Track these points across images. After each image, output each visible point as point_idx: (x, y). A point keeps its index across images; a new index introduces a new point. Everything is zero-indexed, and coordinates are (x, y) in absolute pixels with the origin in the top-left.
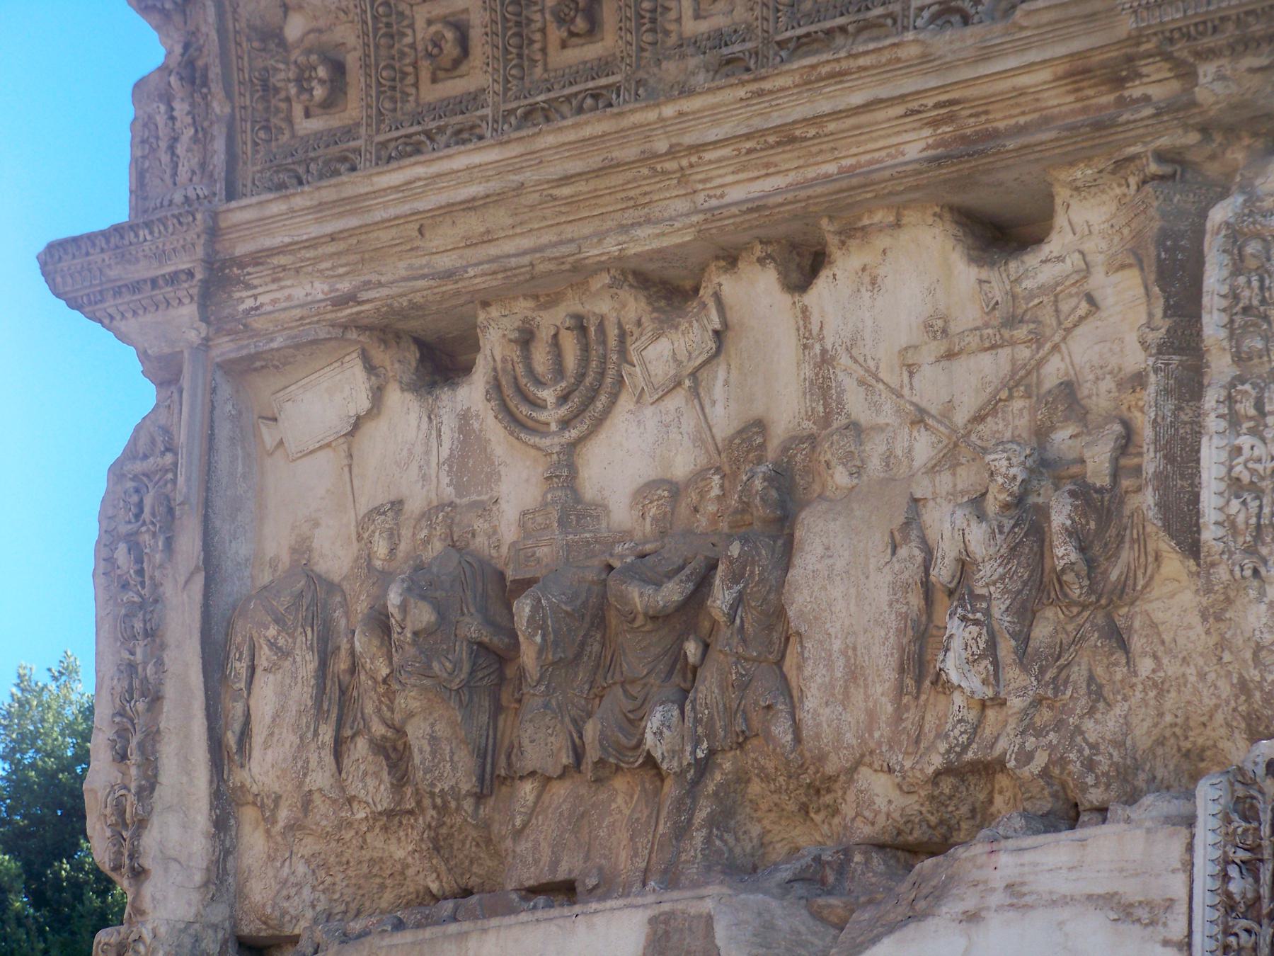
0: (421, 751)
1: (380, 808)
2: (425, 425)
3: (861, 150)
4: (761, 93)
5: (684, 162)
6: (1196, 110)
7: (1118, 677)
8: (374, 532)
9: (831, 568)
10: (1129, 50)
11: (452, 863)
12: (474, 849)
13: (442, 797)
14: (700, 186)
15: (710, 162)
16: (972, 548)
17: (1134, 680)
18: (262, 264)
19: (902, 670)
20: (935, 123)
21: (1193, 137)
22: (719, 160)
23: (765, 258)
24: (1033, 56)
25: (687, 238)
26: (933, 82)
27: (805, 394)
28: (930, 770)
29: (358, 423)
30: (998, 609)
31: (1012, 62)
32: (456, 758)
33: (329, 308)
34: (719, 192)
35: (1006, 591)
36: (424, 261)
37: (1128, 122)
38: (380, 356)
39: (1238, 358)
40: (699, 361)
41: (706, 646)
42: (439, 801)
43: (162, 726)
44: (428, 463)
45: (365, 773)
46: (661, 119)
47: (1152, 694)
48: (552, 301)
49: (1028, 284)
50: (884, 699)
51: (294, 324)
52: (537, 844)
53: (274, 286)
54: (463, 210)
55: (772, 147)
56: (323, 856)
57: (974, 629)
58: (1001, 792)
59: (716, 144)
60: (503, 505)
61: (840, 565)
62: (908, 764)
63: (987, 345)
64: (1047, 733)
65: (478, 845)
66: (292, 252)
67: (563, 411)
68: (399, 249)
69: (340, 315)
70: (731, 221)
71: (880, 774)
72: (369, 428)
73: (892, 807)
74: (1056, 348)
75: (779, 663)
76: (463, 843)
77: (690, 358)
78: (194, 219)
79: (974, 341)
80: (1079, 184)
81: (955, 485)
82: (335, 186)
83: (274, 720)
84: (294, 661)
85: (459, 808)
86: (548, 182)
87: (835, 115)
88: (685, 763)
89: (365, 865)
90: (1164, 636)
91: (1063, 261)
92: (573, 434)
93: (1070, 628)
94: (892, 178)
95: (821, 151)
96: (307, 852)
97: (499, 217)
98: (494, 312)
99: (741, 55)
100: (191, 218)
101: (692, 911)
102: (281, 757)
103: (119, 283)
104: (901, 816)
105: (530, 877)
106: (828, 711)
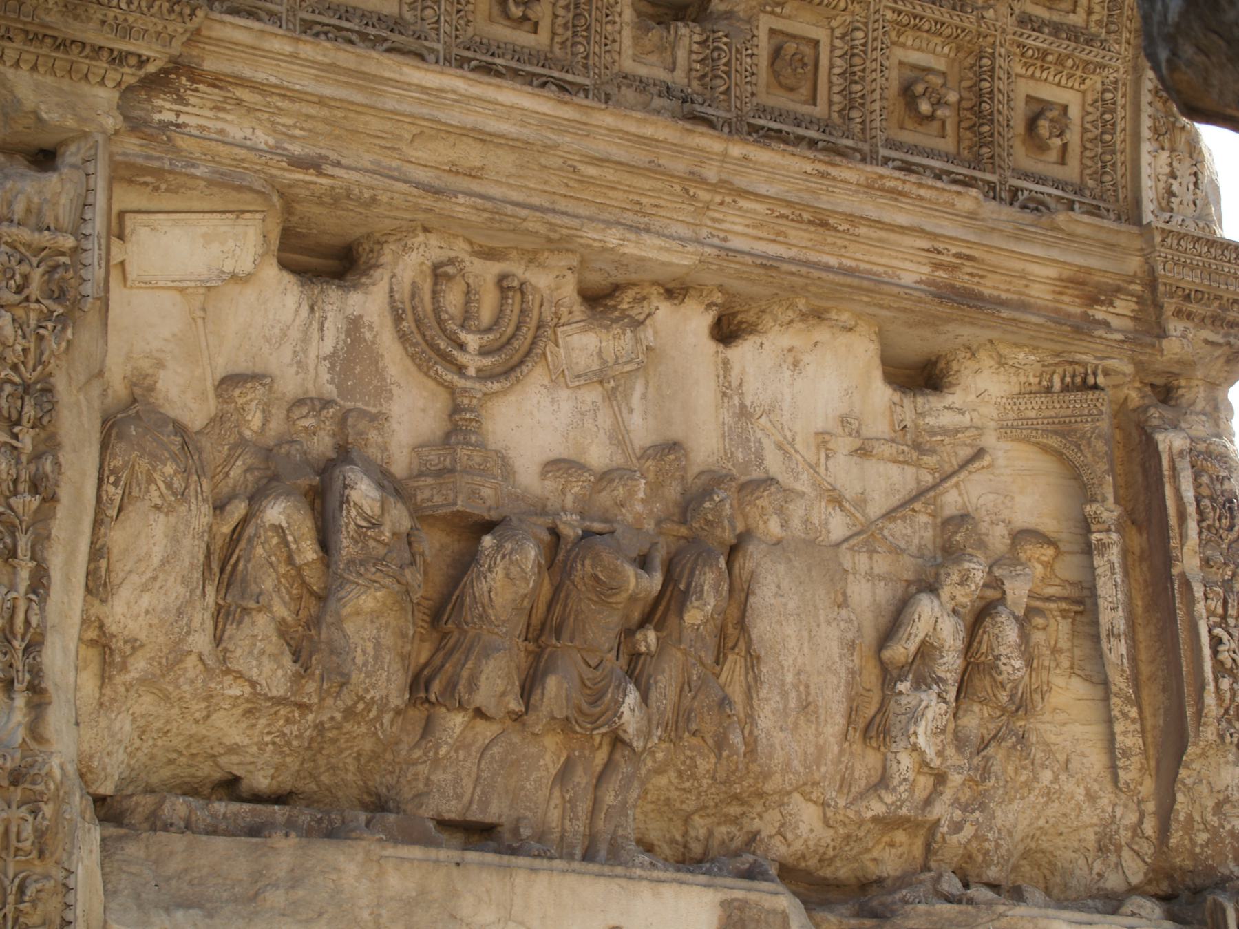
0: (364, 652)
1: (274, 693)
3: (866, 258)
4: (824, 175)
5: (718, 199)
6: (1149, 350)
7: (1023, 778)
8: (251, 400)
9: (785, 605)
10: (1123, 284)
11: (306, 766)
12: (349, 760)
13: (367, 704)
14: (709, 223)
15: (740, 208)
17: (1035, 785)
18: (221, 88)
20: (937, 266)
22: (747, 211)
23: (716, 305)
25: (686, 263)
26: (971, 238)
27: (723, 436)
28: (869, 814)
31: (1039, 251)
32: (391, 671)
33: (284, 165)
34: (722, 235)
36: (395, 164)
37: (1100, 337)
39: (1206, 562)
40: (628, 368)
42: (361, 706)
43: (54, 532)
44: (305, 351)
45: (263, 652)
46: (725, 154)
47: (1042, 800)
48: (490, 254)
49: (930, 420)
50: (832, 740)
51: (228, 162)
52: (457, 779)
53: (210, 114)
54: (475, 139)
55: (802, 222)
56: (151, 719)
58: (891, 845)
59: (757, 197)
60: (395, 426)
61: (791, 605)
62: (842, 803)
63: (901, 458)
64: (973, 811)
65: (357, 759)
66: (263, 96)
68: (377, 141)
69: (287, 175)
70: (737, 266)
71: (810, 804)
73: (812, 836)
74: (957, 485)
76: (341, 751)
77: (616, 362)
78: (192, 14)
81: (872, 568)
82: (358, 56)
83: (163, 564)
84: (190, 510)
85: (379, 718)
86: (582, 155)
88: (649, 745)
89: (180, 738)
90: (1058, 755)
91: (963, 414)
93: (991, 726)
94: (897, 296)
95: (834, 244)
96: (137, 709)
97: (505, 161)
98: (434, 240)
99: (714, 119)
100: (187, 11)
101: (767, 905)
102: (161, 606)
103: (50, 33)
104: (816, 845)
105: (452, 811)
106: (782, 735)
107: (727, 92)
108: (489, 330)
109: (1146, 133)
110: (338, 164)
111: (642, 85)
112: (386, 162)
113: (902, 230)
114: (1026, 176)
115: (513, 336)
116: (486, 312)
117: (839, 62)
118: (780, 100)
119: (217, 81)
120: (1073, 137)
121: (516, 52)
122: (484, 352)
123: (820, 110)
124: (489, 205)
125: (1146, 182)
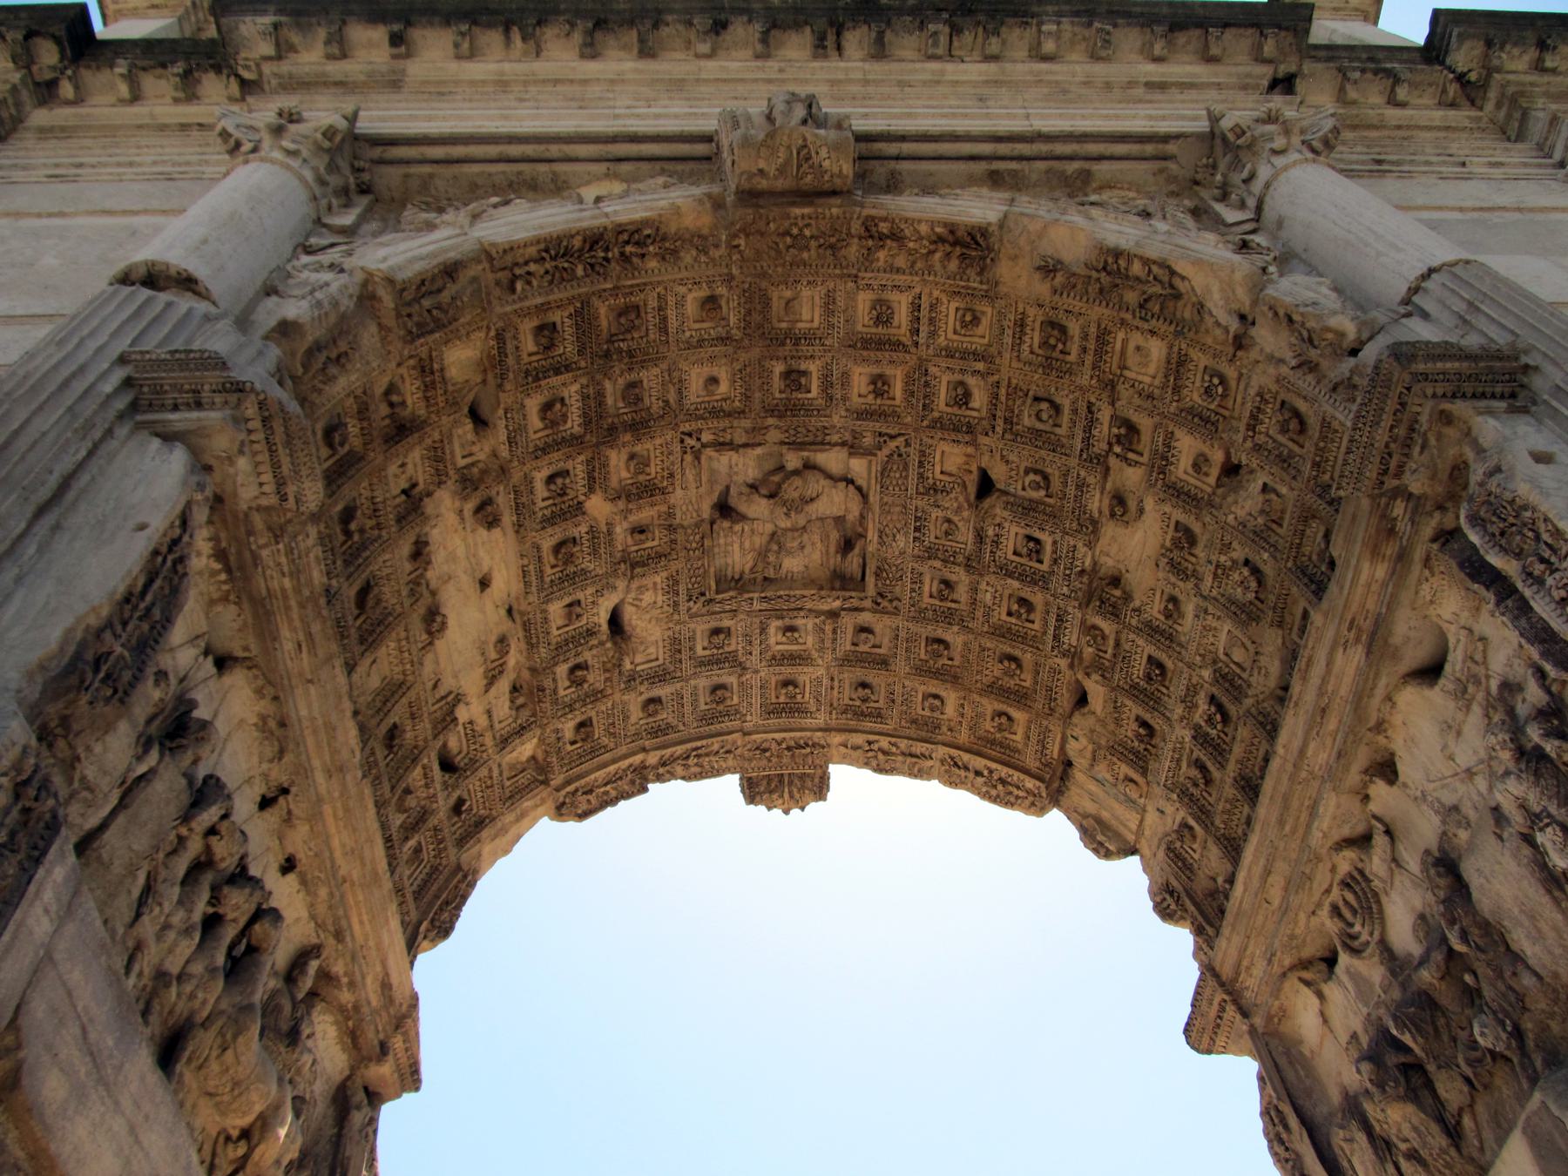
4: (1296, 704)
16: (1515, 792)
19: (1549, 892)
20: (1357, 640)
21: (1437, 515)
24: (1353, 562)
29: (1322, 1014)
30: (1553, 809)
35: (1550, 798)
38: (1306, 975)
39: (1519, 555)
41: (1475, 974)
49: (1458, 667)
57: (1549, 830)
72: (1327, 1013)
75: (1508, 948)
79: (1460, 716)
80: (1428, 598)
87: (1324, 681)
92: (1377, 934)
97: (1281, 867)
113: (1329, 664)
119: (1238, 974)
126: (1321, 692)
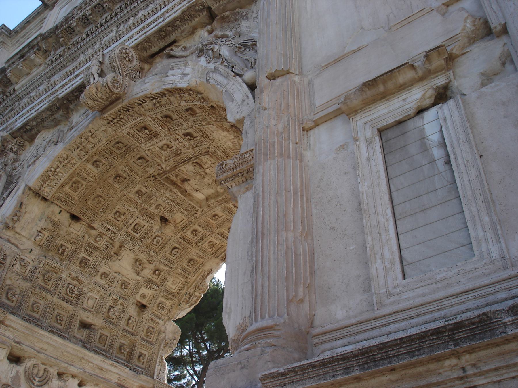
2: (9, 368)
4: (104, 362)
20: (119, 380)
48: (44, 364)
59: (92, 363)
67: (39, 383)
98: (35, 360)
107: (91, 343)
108: (40, 378)
109: (158, 362)
110: (23, 344)
111: (77, 339)
112: (31, 345)
113: (115, 373)
114: (137, 366)
115: (44, 380)
116: (41, 374)
117: (110, 340)
118: (99, 345)
119: (6, 326)
120: (145, 360)
121: (57, 329)
122: (39, 381)
123: (105, 348)
124: (47, 356)
125: (156, 371)
126: (107, 370)
